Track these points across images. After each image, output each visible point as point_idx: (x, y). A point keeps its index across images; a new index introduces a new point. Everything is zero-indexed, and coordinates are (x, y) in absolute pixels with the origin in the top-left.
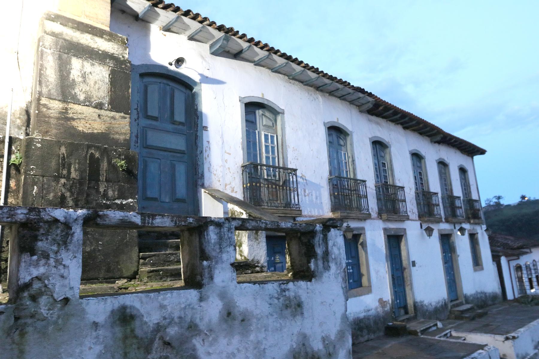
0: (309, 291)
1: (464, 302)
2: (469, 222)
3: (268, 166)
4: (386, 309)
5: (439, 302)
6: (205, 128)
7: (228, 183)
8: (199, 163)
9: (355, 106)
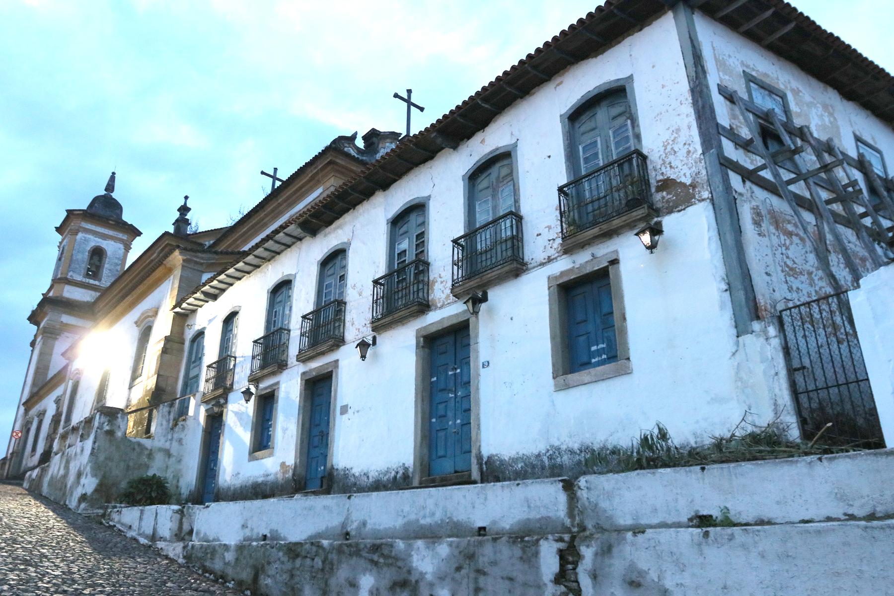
1: (475, 474)
5: (388, 472)
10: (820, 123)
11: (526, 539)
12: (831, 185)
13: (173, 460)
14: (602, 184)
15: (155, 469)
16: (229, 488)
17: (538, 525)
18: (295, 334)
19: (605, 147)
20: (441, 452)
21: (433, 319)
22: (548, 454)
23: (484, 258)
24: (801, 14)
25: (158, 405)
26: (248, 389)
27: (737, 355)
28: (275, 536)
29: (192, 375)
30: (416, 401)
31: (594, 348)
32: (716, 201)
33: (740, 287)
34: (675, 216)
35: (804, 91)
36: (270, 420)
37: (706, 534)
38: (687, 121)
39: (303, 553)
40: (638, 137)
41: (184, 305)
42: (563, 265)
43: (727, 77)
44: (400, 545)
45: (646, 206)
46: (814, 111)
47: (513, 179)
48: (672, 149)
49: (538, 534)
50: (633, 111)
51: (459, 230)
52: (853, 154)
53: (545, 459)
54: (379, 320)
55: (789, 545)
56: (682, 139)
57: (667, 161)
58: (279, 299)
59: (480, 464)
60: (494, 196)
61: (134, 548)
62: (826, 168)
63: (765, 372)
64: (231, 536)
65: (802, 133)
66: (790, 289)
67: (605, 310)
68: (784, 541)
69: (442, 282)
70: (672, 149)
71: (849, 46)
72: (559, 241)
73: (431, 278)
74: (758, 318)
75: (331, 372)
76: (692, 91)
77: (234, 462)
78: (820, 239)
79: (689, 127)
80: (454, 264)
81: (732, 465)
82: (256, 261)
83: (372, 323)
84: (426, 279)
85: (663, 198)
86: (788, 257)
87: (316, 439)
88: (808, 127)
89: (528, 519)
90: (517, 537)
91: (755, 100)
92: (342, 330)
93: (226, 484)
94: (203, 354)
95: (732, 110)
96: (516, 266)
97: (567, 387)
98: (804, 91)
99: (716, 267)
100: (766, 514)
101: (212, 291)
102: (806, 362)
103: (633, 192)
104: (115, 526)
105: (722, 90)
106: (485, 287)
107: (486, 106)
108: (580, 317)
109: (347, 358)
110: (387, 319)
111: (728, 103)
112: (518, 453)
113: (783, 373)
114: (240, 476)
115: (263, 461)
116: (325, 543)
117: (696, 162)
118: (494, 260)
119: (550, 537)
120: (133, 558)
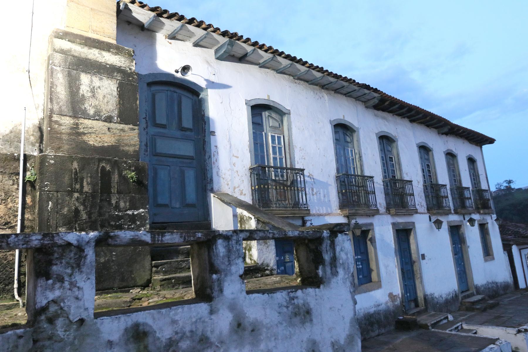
0: (317, 297)
2: (479, 213)
3: (275, 168)
4: (396, 303)
5: (449, 294)
6: (213, 133)
7: (237, 185)
8: (208, 168)
9: (361, 102)
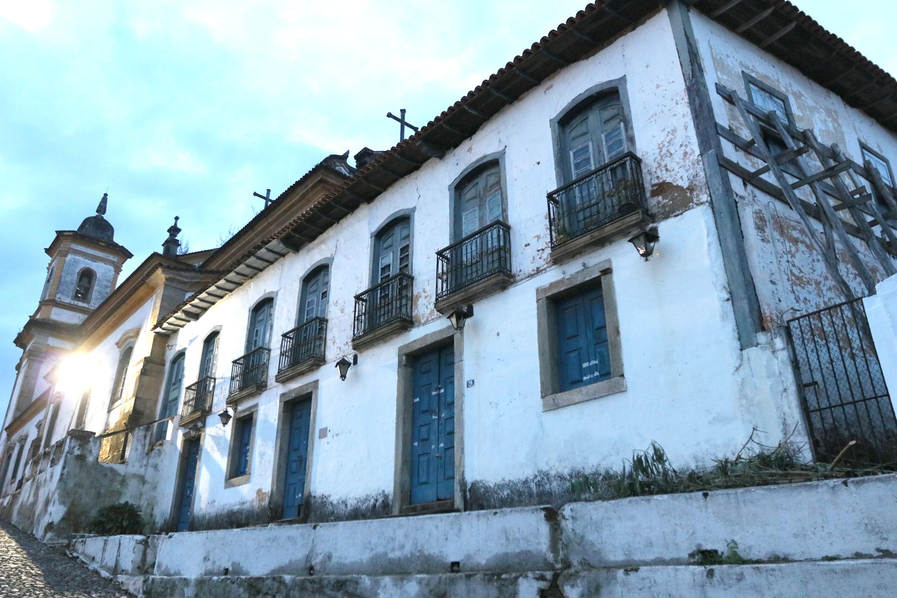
1: (458, 502)
5: (367, 499)
10: (823, 128)
11: (504, 576)
12: (838, 191)
13: (147, 486)
14: (594, 188)
15: (128, 497)
16: (204, 517)
17: (517, 560)
18: (275, 353)
19: (597, 155)
20: (423, 479)
21: (416, 335)
22: (536, 481)
23: (469, 271)
24: (802, 13)
25: (134, 429)
26: (226, 412)
27: (741, 371)
28: (237, 570)
29: (171, 397)
30: (397, 423)
31: (585, 365)
32: (716, 205)
33: (743, 296)
34: (671, 221)
35: (806, 95)
36: (247, 444)
37: (711, 574)
38: (683, 121)
39: (265, 590)
40: (631, 140)
41: (165, 325)
42: (553, 276)
43: (725, 77)
44: (366, 581)
45: (640, 211)
46: (817, 116)
47: (501, 188)
48: (668, 151)
49: (517, 571)
50: (626, 113)
51: (444, 241)
52: (859, 161)
53: (533, 485)
54: (360, 337)
55: (811, 586)
56: (678, 140)
57: (663, 164)
58: (260, 318)
59: (464, 491)
60: (481, 207)
61: (93, 582)
62: (832, 172)
63: (771, 388)
64: (192, 571)
65: (805, 137)
66: (797, 300)
67: (597, 324)
68: (805, 583)
69: (426, 297)
70: (668, 151)
71: (852, 49)
72: (549, 251)
73: (415, 293)
74: (763, 329)
75: (311, 393)
76: (689, 90)
77: (210, 490)
78: (829, 247)
79: (686, 128)
80: (438, 277)
81: (740, 490)
82: (237, 279)
83: (353, 340)
84: (409, 294)
85: (659, 202)
86: (794, 265)
87: (294, 465)
88: (812, 132)
89: (507, 553)
90: (493, 575)
91: (755, 102)
92: (323, 349)
93: (201, 513)
94: (183, 376)
95: (731, 110)
96: (503, 278)
97: (556, 407)
98: (806, 95)
99: (716, 275)
100: (782, 549)
101: (194, 310)
102: (818, 377)
103: (627, 198)
104: (78, 557)
105: (720, 89)
106: (471, 300)
107: (473, 112)
108: (570, 331)
109: (327, 378)
110: (368, 337)
111: (727, 103)
112: (503, 479)
113: (792, 389)
114: (216, 504)
115: (240, 487)
116: (287, 578)
117: (693, 164)
118: (480, 272)
119: (530, 574)
120: (89, 593)
